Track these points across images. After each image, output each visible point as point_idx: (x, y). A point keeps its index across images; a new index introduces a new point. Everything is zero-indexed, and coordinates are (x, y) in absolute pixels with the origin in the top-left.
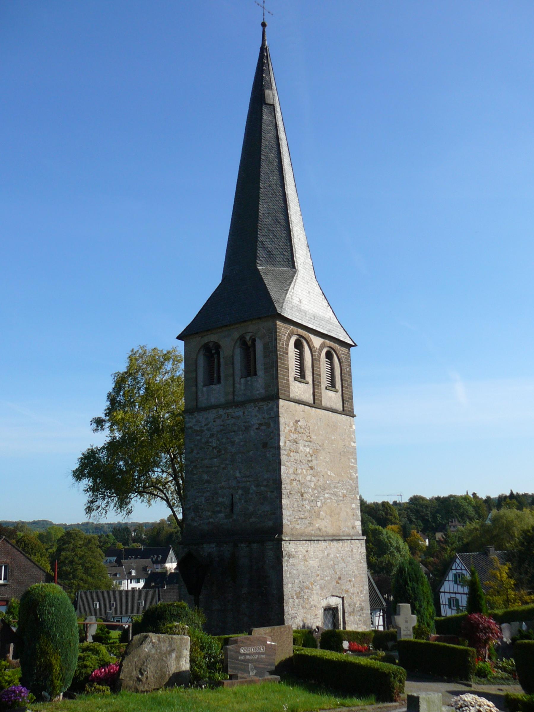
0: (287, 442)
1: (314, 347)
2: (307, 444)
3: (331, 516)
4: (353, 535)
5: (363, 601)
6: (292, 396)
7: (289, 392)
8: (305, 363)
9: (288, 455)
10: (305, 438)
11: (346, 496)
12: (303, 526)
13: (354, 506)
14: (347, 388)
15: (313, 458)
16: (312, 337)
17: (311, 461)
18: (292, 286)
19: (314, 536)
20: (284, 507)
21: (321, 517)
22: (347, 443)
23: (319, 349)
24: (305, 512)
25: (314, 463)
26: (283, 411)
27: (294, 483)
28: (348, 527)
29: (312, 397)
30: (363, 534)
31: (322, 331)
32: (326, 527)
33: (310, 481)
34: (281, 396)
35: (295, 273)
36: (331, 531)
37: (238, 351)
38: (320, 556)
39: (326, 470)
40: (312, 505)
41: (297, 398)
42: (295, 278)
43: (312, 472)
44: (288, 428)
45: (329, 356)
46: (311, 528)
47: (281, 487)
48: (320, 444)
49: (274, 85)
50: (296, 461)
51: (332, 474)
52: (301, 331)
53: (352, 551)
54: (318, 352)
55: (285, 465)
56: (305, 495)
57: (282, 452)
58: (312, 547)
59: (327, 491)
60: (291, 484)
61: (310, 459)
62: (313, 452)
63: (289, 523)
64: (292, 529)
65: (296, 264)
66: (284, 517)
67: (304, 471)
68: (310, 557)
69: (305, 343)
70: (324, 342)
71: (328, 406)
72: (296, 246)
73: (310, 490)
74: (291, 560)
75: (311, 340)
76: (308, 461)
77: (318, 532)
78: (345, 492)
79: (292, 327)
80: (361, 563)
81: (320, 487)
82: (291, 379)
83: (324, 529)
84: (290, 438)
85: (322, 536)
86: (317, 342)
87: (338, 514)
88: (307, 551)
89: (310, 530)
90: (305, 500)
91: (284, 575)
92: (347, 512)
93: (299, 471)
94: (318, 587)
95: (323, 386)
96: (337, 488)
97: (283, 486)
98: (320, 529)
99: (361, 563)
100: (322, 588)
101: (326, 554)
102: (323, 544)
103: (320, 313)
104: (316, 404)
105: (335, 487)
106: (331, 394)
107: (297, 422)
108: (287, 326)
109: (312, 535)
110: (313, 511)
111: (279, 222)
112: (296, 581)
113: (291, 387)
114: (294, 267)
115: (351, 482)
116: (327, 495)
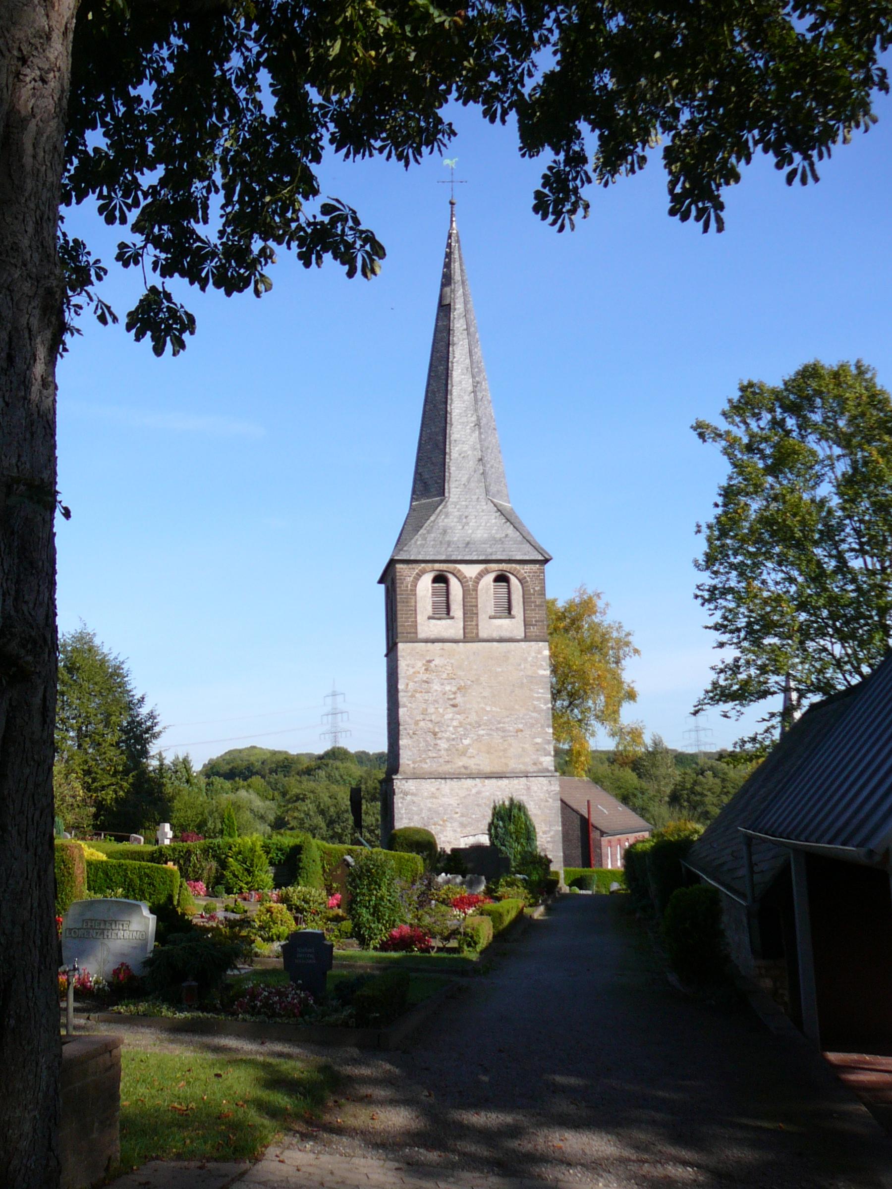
0: (411, 684)
2: (446, 682)
3: (488, 753)
4: (534, 772)
5: (548, 842)
6: (422, 635)
7: (416, 633)
8: (451, 597)
9: (413, 696)
10: (445, 676)
11: (522, 731)
12: (434, 765)
13: (539, 740)
14: (534, 610)
15: (458, 695)
16: (459, 566)
17: (455, 698)
18: (432, 518)
19: (454, 774)
20: (401, 747)
21: (468, 754)
22: (530, 673)
23: (476, 578)
24: (439, 750)
25: (459, 700)
26: (403, 654)
27: (422, 724)
28: (524, 764)
29: (462, 631)
30: (556, 771)
31: (475, 558)
33: (452, 719)
34: (398, 640)
35: (442, 501)
36: (487, 769)
38: (462, 793)
39: (482, 705)
40: (454, 743)
41: (432, 637)
42: (440, 508)
43: (455, 709)
44: (411, 671)
45: (501, 578)
46: (449, 766)
47: (399, 730)
48: (474, 679)
49: (457, 277)
50: (426, 701)
51: (494, 709)
52: (437, 566)
53: (529, 788)
54: (475, 582)
55: (405, 706)
56: (439, 735)
57: (401, 694)
58: (446, 786)
59: (483, 727)
60: (417, 723)
61: (452, 696)
62: (459, 689)
63: (410, 762)
64: (414, 768)
65: (446, 491)
66: (401, 756)
67: (441, 710)
68: (443, 796)
69: (450, 576)
70: (486, 569)
71: (495, 635)
72: (453, 469)
73: (451, 729)
74: (409, 798)
75: (459, 571)
76: (449, 699)
77: (463, 770)
78: (521, 726)
79: (423, 565)
80: (547, 801)
81: (470, 724)
82: (421, 618)
83: (474, 767)
84: (416, 679)
85: (471, 774)
86: (471, 571)
87: (505, 750)
88: (438, 789)
89: (447, 768)
90: (440, 739)
91: (396, 810)
92: (523, 748)
93: (431, 710)
94: (456, 824)
95: (483, 618)
96: (504, 723)
97: (401, 728)
98: (466, 768)
99: (547, 801)
100: (463, 825)
101: (474, 791)
102: (469, 781)
103: (486, 535)
104: (470, 636)
105: (499, 723)
106: (505, 622)
107: (430, 661)
108: (414, 566)
109: (450, 773)
110: (454, 750)
111: (437, 446)
112: (416, 817)
113: (419, 628)
115: (535, 715)
116: (482, 732)
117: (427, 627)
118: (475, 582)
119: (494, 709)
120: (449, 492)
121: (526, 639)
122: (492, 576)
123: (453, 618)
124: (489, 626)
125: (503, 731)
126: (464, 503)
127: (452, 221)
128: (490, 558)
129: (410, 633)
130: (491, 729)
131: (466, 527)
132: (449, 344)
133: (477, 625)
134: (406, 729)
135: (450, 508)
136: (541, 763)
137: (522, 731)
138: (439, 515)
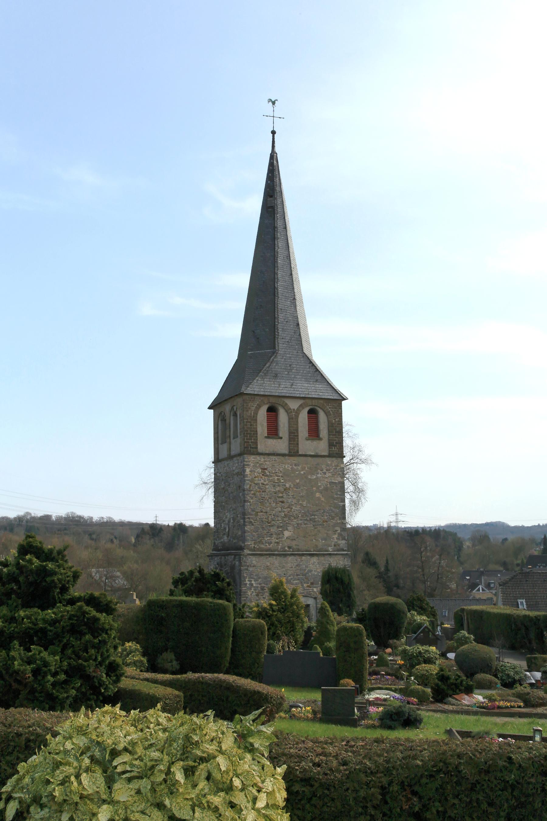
1: (290, 409)
3: (305, 537)
7: (257, 448)
11: (326, 521)
14: (335, 435)
16: (287, 401)
18: (267, 365)
32: (298, 545)
35: (274, 353)
37: (232, 417)
54: (296, 412)
58: (276, 561)
60: (256, 514)
75: (286, 404)
83: (295, 547)
86: (294, 405)
92: (327, 534)
106: (315, 443)
114: (274, 348)
117: (265, 444)
118: (296, 412)
119: (308, 505)
120: (278, 346)
121: (330, 456)
122: (306, 410)
123: (281, 438)
124: (307, 446)
125: (315, 522)
126: (288, 355)
127: (273, 146)
128: (307, 396)
129: (253, 448)
130: (306, 520)
131: (290, 373)
132: (274, 238)
133: (298, 444)
134: (249, 518)
135: (279, 358)
136: (339, 545)
137: (326, 521)
138: (272, 362)
